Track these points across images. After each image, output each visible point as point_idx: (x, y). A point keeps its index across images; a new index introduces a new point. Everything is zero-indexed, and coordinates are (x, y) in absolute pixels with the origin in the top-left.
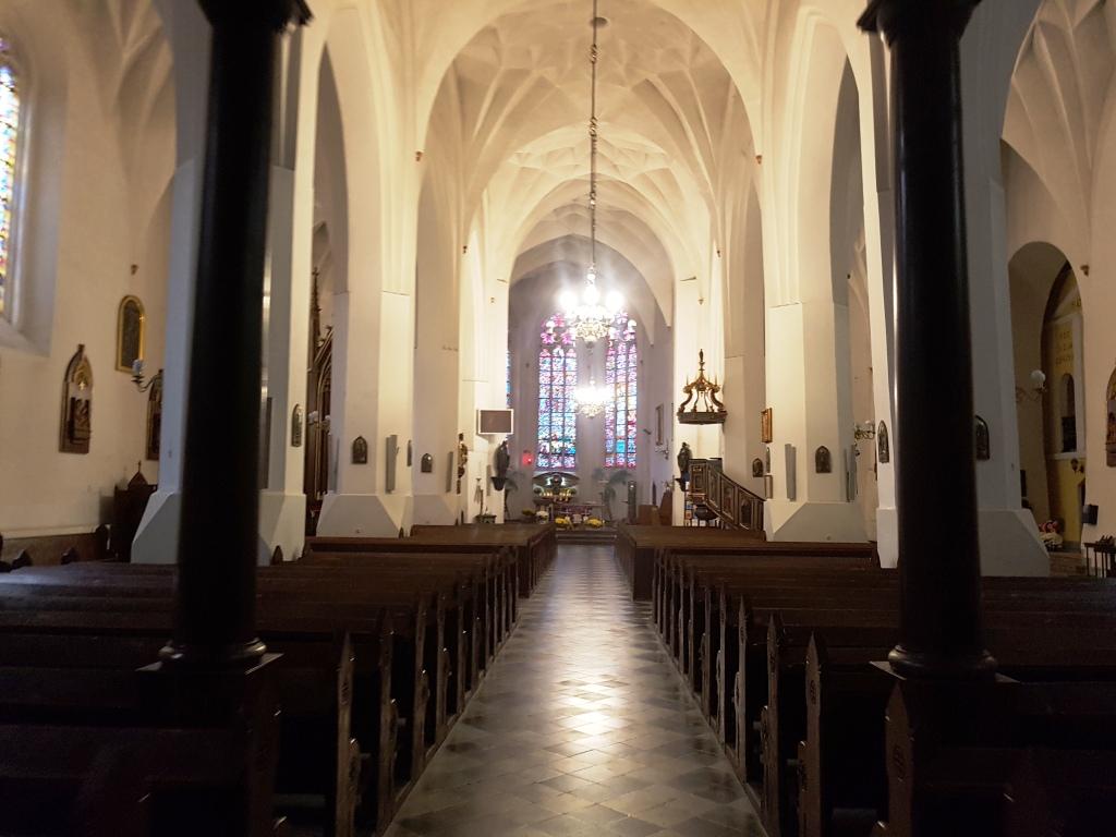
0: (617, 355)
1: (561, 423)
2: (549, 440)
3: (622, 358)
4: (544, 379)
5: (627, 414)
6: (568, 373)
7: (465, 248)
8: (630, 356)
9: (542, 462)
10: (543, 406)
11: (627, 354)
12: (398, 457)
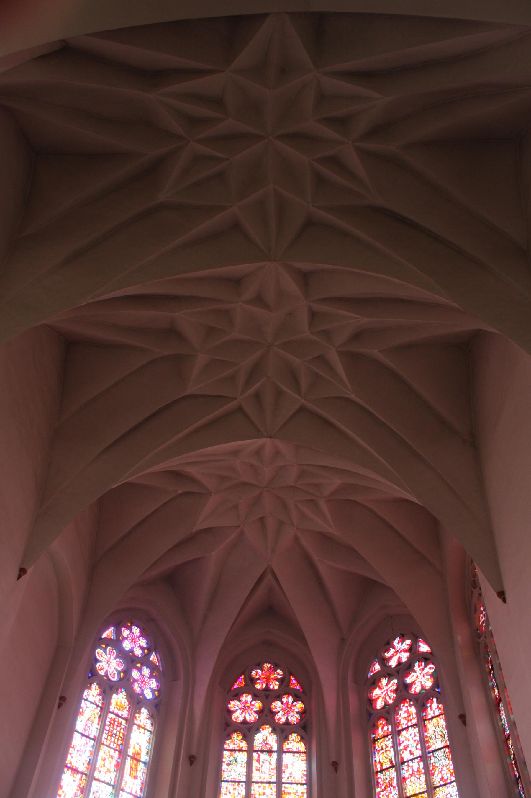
0: (397, 733)
3: (410, 737)
6: (286, 788)
8: (430, 725)
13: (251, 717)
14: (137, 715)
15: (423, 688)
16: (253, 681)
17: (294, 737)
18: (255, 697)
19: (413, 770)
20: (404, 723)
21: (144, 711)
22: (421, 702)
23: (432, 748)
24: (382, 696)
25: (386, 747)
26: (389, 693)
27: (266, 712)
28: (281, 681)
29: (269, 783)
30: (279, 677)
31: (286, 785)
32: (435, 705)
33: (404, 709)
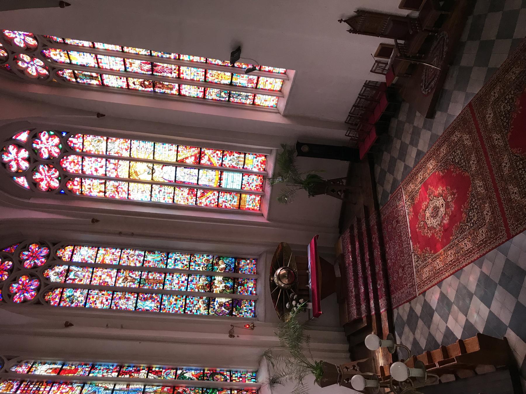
0: (83, 176)
3: (90, 166)
4: (100, 301)
5: (180, 164)
8: (88, 147)
9: (246, 311)
10: (149, 305)
11: (84, 155)
15: (57, 146)
17: (60, 253)
19: (114, 169)
20: (78, 167)
22: (67, 150)
23: (104, 150)
24: (49, 180)
25: (90, 185)
26: (50, 174)
29: (93, 273)
31: (97, 260)
32: (75, 140)
33: (67, 165)
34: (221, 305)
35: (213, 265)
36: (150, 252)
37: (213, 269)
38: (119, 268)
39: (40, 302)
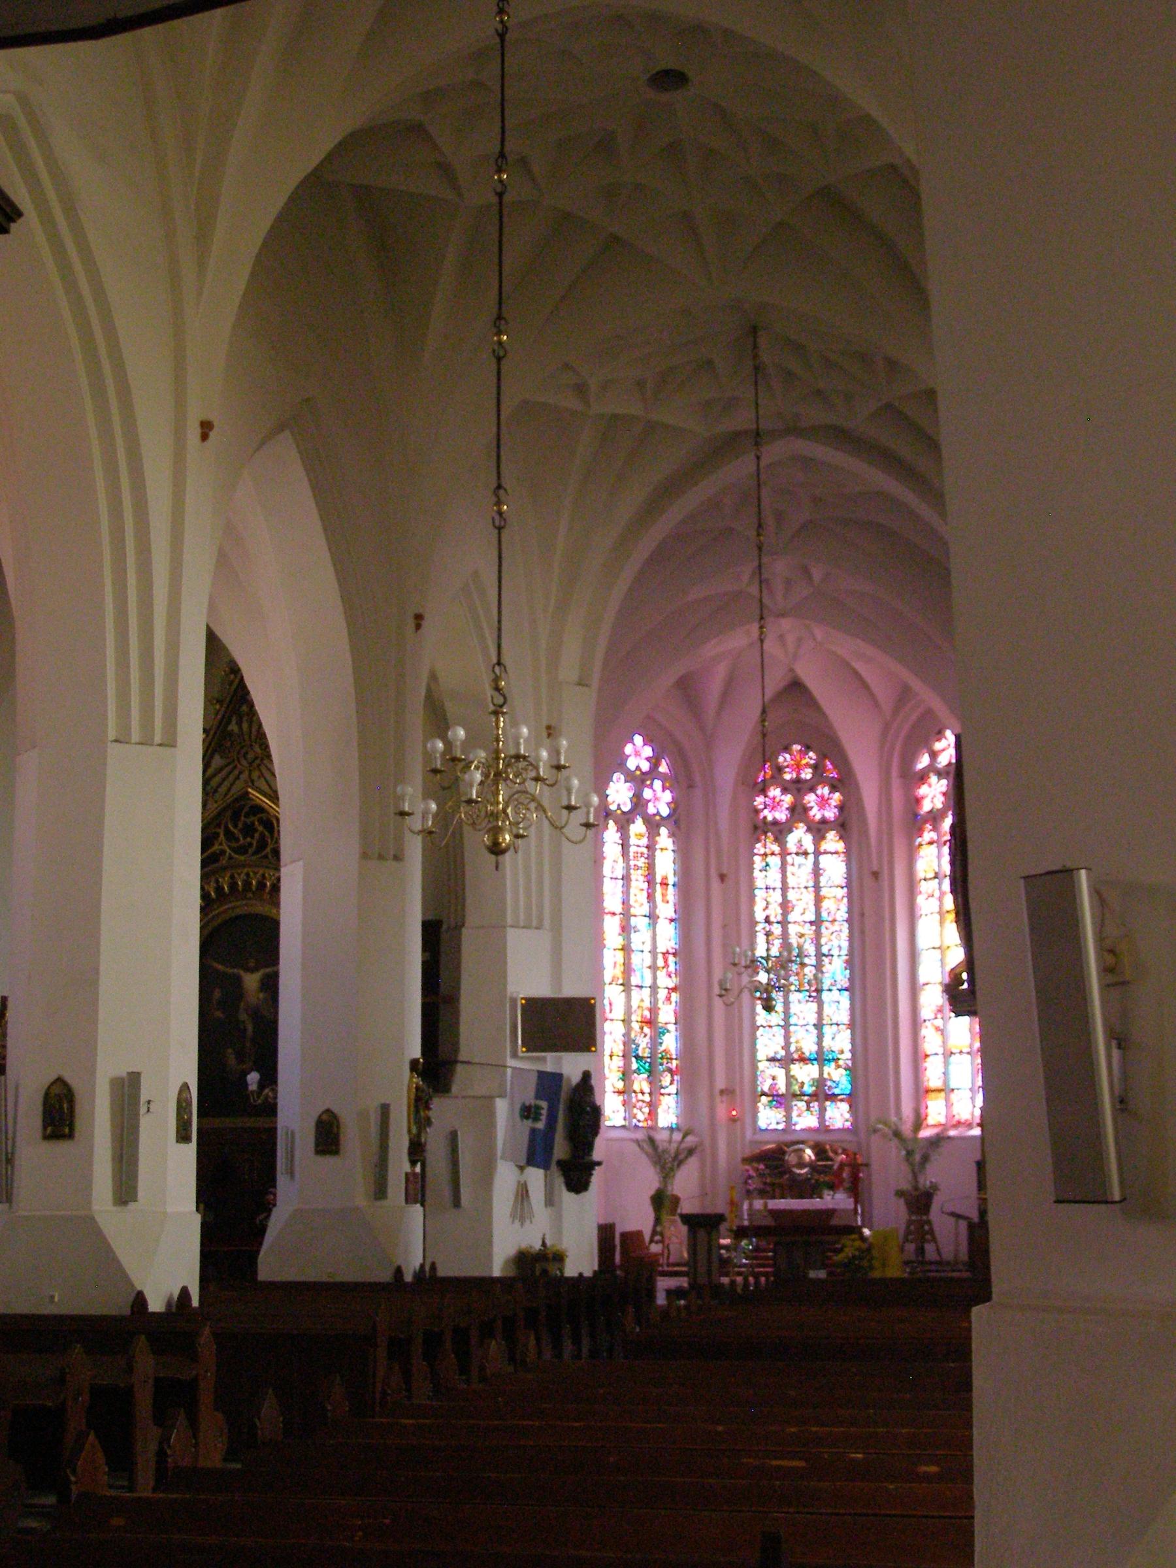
1: (813, 1019)
2: (786, 1061)
6: (824, 892)
7: (419, 617)
12: (145, 1122)
13: (781, 815)
14: (657, 838)
16: (780, 770)
18: (785, 790)
21: (664, 831)
27: (799, 810)
28: (815, 767)
30: (812, 762)
34: (774, 1078)
35: (836, 1060)
36: (847, 962)
37: (829, 1060)
38: (817, 923)
39: (760, 828)
